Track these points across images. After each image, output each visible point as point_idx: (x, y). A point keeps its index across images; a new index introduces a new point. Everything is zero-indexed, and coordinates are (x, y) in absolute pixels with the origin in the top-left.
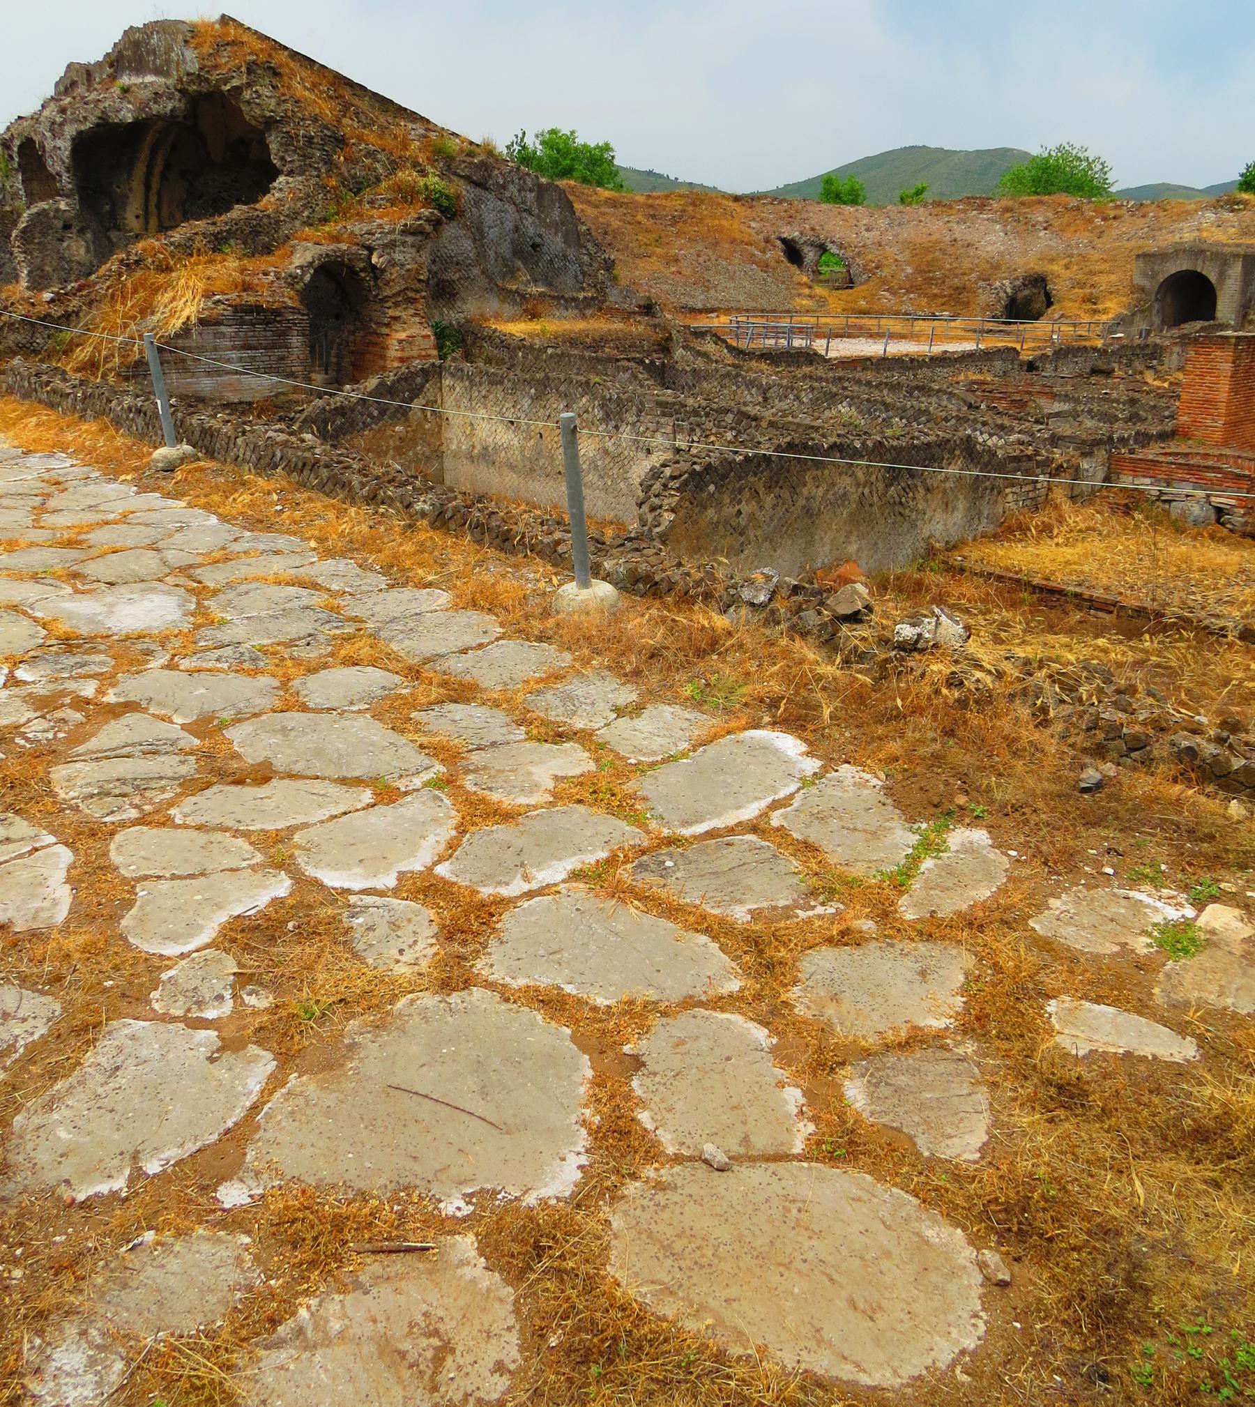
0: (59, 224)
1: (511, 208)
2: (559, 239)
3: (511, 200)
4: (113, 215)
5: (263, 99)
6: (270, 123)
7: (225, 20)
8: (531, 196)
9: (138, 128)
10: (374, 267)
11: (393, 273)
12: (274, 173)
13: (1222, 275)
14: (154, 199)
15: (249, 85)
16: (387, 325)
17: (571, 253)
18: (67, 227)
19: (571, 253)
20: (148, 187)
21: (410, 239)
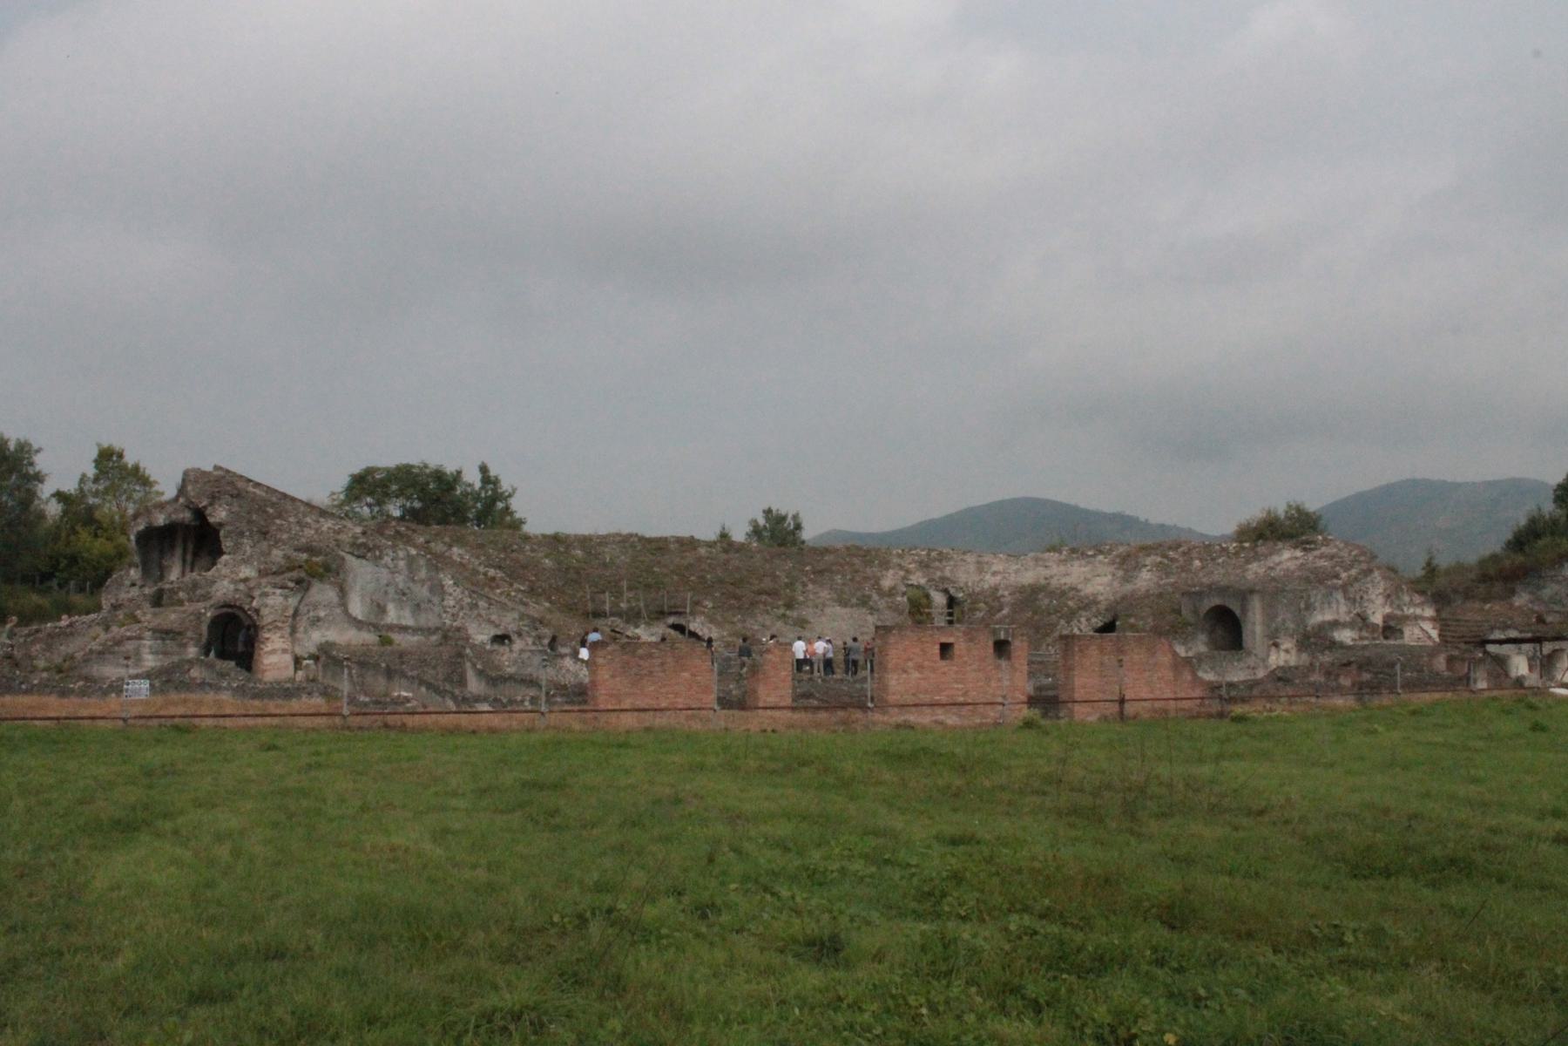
1: (385, 571)
3: (386, 566)
5: (219, 514)
6: (221, 525)
7: (217, 468)
8: (402, 564)
11: (264, 611)
12: (221, 553)
15: (211, 504)
19: (436, 600)
21: (278, 591)
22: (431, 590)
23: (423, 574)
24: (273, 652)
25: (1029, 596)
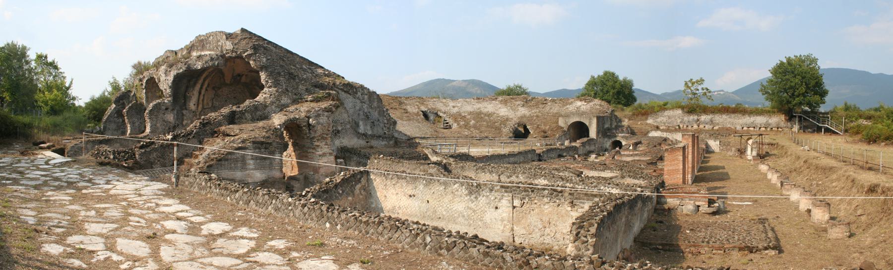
0: (164, 108)
1: (358, 101)
2: (376, 114)
3: (358, 98)
4: (185, 104)
9: (203, 70)
10: (309, 125)
11: (319, 127)
13: (590, 122)
14: (201, 98)
16: (314, 149)
17: (381, 119)
18: (167, 109)
20: (200, 93)
21: (326, 114)
22: (379, 114)
23: (375, 104)
24: (324, 155)
25: (478, 115)
